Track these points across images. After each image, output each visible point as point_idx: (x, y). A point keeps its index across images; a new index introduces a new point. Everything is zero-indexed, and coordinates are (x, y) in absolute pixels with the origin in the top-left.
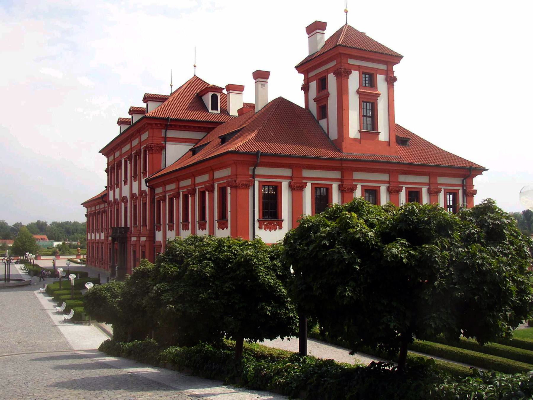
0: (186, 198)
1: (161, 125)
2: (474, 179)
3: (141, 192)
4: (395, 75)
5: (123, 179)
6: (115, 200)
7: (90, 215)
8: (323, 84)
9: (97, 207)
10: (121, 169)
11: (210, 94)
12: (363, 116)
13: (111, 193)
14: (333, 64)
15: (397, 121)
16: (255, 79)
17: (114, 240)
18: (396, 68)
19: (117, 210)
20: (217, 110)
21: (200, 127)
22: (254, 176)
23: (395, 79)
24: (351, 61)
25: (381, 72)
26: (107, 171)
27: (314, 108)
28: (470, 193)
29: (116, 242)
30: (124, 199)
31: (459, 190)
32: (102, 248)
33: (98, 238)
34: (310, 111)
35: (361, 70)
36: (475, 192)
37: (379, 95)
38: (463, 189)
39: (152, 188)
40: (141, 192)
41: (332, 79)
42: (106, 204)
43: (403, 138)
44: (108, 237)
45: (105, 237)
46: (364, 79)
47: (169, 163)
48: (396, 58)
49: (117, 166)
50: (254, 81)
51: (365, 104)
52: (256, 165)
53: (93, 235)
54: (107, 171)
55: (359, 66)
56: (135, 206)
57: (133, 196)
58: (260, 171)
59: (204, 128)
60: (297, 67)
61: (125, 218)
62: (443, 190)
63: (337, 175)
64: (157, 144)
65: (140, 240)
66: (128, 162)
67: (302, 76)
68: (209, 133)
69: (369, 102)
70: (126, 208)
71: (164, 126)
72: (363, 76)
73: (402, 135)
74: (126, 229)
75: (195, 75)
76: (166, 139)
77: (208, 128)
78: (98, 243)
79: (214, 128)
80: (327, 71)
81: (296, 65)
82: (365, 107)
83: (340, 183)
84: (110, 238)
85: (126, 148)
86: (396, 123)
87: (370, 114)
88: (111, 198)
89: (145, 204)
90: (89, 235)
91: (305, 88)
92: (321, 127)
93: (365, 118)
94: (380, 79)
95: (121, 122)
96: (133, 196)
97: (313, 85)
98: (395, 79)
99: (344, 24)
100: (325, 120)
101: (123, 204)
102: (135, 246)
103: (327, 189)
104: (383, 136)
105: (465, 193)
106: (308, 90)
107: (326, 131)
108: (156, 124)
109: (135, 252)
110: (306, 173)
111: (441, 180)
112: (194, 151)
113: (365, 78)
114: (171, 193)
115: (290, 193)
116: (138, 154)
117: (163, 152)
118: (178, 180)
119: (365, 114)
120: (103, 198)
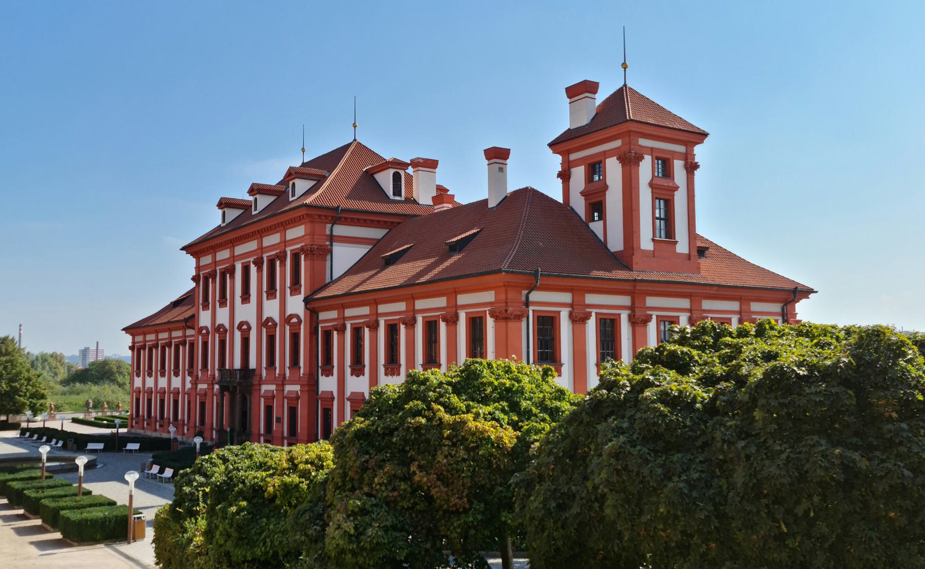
1: (326, 216)
4: (696, 160)
11: (391, 172)
12: (657, 218)
18: (698, 149)
21: (378, 221)
23: (696, 166)
27: (579, 205)
34: (573, 209)
35: (655, 155)
40: (287, 320)
59: (385, 222)
77: (392, 223)
80: (606, 154)
82: (657, 206)
91: (565, 175)
92: (593, 232)
94: (678, 166)
95: (224, 204)
98: (696, 166)
104: (682, 247)
108: (319, 216)
117: (329, 257)
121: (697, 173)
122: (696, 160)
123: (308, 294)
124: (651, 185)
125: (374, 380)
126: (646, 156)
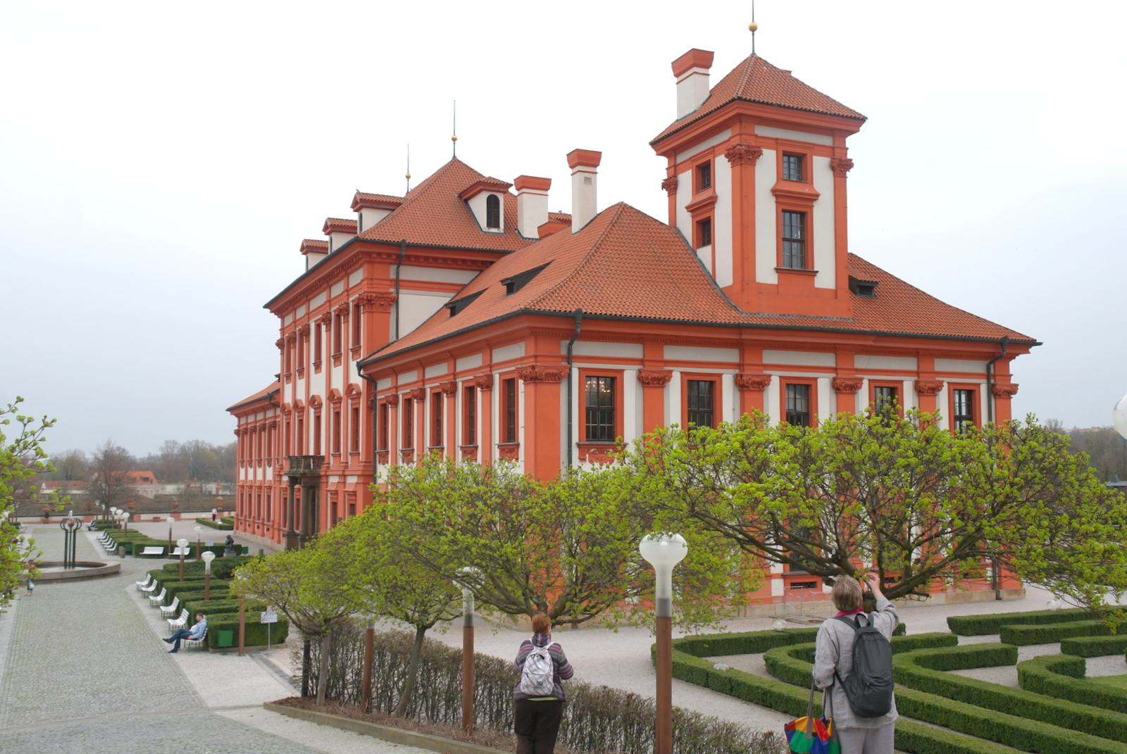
0: (437, 398)
2: (1012, 363)
3: (349, 388)
4: (849, 157)
5: (312, 360)
6: (296, 405)
7: (245, 431)
8: (704, 175)
9: (260, 416)
10: (308, 341)
12: (784, 239)
13: (288, 388)
14: (725, 136)
15: (851, 249)
16: (572, 167)
17: (294, 480)
18: (850, 141)
19: (301, 421)
20: (497, 226)
21: (464, 261)
22: (569, 358)
23: (848, 165)
24: (761, 131)
25: (822, 150)
26: (280, 344)
27: (686, 225)
28: (1003, 392)
29: (297, 486)
30: (314, 402)
31: (979, 385)
32: (269, 497)
33: (260, 477)
34: (679, 232)
36: (1013, 390)
37: (816, 196)
38: (989, 382)
39: (371, 381)
40: (349, 388)
41: (723, 169)
42: (278, 412)
43: (864, 283)
44: (281, 476)
45: (274, 476)
46: (786, 165)
47: (402, 334)
48: (854, 121)
49: (301, 335)
50: (571, 171)
51: (787, 215)
52: (573, 337)
53: (251, 471)
54: (280, 344)
55: (777, 139)
56: (337, 414)
57: (332, 395)
58: (581, 348)
59: (473, 262)
60: (654, 144)
61: (317, 439)
62: (945, 385)
63: (732, 356)
64: (382, 294)
65: (345, 483)
66: (323, 327)
67: (664, 161)
68: (482, 271)
69: (796, 211)
70: (318, 418)
71: (394, 257)
72: (786, 158)
73: (861, 276)
74: (318, 459)
75: (454, 157)
76: (398, 283)
77: (483, 263)
78: (260, 487)
79: (492, 263)
80: (713, 151)
81: (652, 137)
82: (787, 223)
83: (737, 371)
84: (285, 479)
85: (319, 301)
86: (850, 250)
87: (797, 235)
88: (288, 399)
89: (356, 411)
90: (242, 471)
91: (670, 185)
93: (787, 244)
94: (820, 167)
95: (309, 248)
96: (332, 395)
97: (686, 180)
99: (748, 54)
100: (708, 249)
101: (312, 411)
102: (336, 493)
103: (712, 383)
104: (826, 278)
105: (993, 392)
106: (676, 188)
107: (710, 270)
108: (379, 254)
109: (334, 504)
110: (671, 353)
111: (941, 365)
112: (453, 309)
113: (789, 162)
114: (408, 391)
115: (640, 390)
116: (343, 312)
117: (393, 310)
118: (422, 365)
119: (787, 236)
120: (270, 400)
121: (850, 174)
122: (849, 157)
123: (366, 357)
124: (775, 192)
125: (544, 464)
126: (765, 151)
